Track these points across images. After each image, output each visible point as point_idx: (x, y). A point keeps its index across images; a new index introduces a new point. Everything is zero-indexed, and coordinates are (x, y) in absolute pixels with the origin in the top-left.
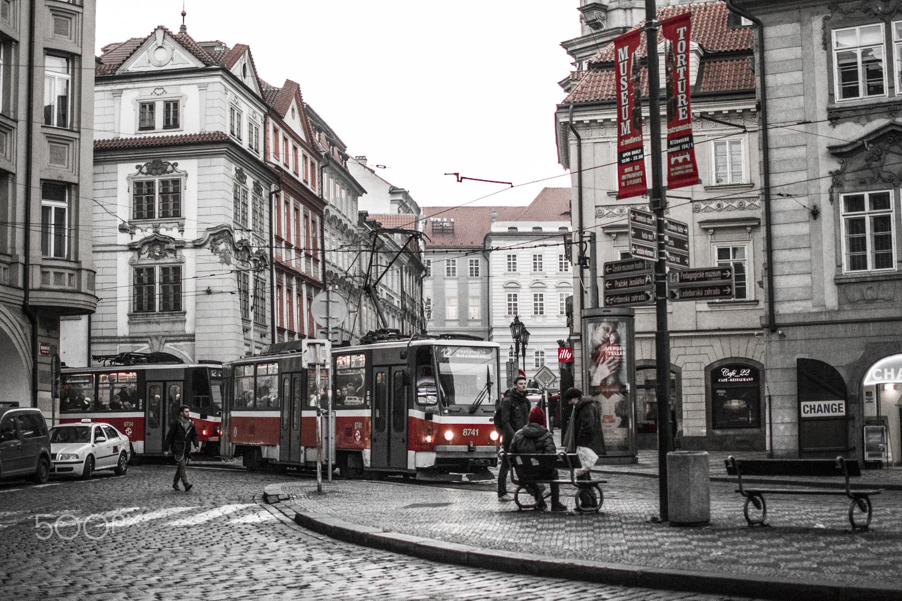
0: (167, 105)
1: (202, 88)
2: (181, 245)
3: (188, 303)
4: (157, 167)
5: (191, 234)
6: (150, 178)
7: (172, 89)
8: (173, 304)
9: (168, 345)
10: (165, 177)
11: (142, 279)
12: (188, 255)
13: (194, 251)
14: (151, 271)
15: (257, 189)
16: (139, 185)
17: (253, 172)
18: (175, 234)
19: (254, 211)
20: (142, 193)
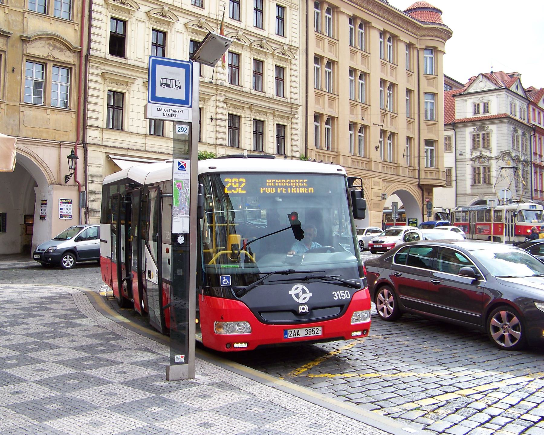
0: (484, 104)
1: (498, 96)
2: (490, 158)
3: (493, 181)
4: (481, 128)
5: (494, 154)
6: (478, 133)
7: (486, 98)
8: (487, 181)
9: (486, 197)
10: (484, 132)
11: (476, 171)
12: (493, 162)
13: (496, 161)
14: (479, 168)
15: (524, 134)
16: (474, 135)
17: (521, 128)
18: (488, 154)
19: (522, 144)
20: (475, 138)
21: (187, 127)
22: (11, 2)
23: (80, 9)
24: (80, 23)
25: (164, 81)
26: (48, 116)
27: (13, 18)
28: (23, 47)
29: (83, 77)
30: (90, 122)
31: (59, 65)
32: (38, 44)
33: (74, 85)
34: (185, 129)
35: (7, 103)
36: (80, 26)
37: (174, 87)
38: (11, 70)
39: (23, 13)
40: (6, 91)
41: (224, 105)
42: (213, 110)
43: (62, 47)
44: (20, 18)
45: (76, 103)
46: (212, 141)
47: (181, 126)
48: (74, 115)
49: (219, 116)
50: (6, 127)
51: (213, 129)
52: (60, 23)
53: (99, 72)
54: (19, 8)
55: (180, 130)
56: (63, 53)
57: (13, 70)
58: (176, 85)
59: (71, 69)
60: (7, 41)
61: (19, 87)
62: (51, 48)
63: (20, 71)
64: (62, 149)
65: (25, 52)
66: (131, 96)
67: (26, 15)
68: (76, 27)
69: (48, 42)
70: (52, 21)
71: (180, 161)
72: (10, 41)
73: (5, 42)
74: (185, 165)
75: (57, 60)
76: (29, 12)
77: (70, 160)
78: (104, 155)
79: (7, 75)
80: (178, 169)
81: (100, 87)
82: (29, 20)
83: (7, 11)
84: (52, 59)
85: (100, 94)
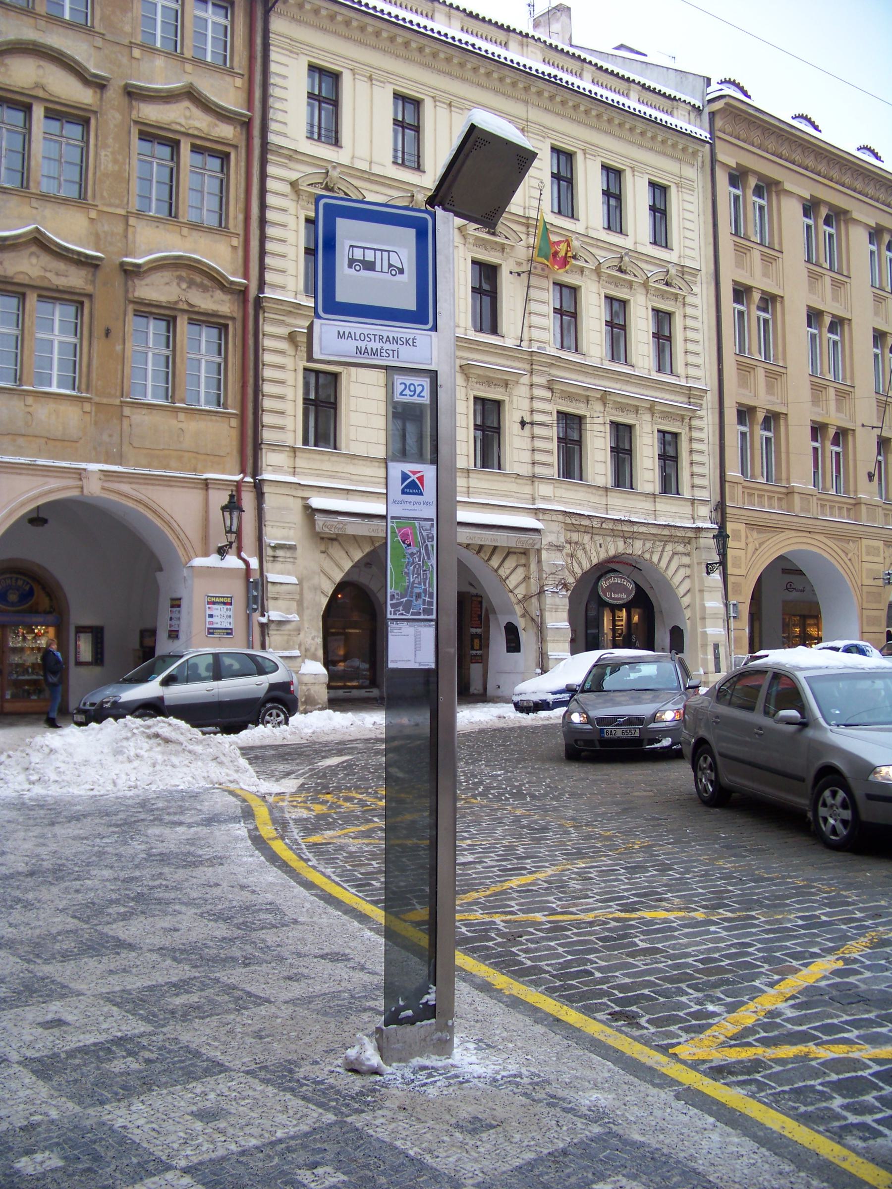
21: (426, 382)
22: (102, 197)
23: (241, 205)
24: (241, 231)
25: (358, 254)
26: (181, 425)
27: (106, 228)
28: (126, 284)
29: (251, 342)
30: (267, 436)
31: (200, 318)
32: (158, 278)
33: (234, 361)
34: (419, 389)
35: (97, 399)
36: (241, 238)
37: (385, 269)
38: (103, 333)
39: (126, 218)
40: (94, 375)
41: (548, 394)
42: (525, 404)
43: (207, 282)
44: (119, 228)
45: (239, 397)
46: (526, 470)
47: (409, 380)
48: (234, 422)
49: (538, 418)
50: (95, 449)
51: (526, 444)
52: (201, 234)
53: (284, 331)
54: (117, 206)
55: (407, 392)
56: (208, 295)
57: (108, 332)
58: (390, 265)
59: (226, 326)
60: (94, 275)
61: (120, 367)
62: (184, 286)
63: (121, 334)
64: (211, 491)
65: (130, 296)
66: (353, 379)
67: (132, 221)
68: (235, 242)
69: (178, 273)
70: (185, 231)
71: (408, 467)
72: (100, 275)
73: (90, 277)
74: (421, 479)
75: (196, 309)
76: (140, 215)
77: (227, 514)
78: (297, 505)
79: (95, 342)
80: (403, 492)
81: (288, 361)
82: (139, 230)
83: (93, 214)
84: (186, 307)
85: (288, 376)
